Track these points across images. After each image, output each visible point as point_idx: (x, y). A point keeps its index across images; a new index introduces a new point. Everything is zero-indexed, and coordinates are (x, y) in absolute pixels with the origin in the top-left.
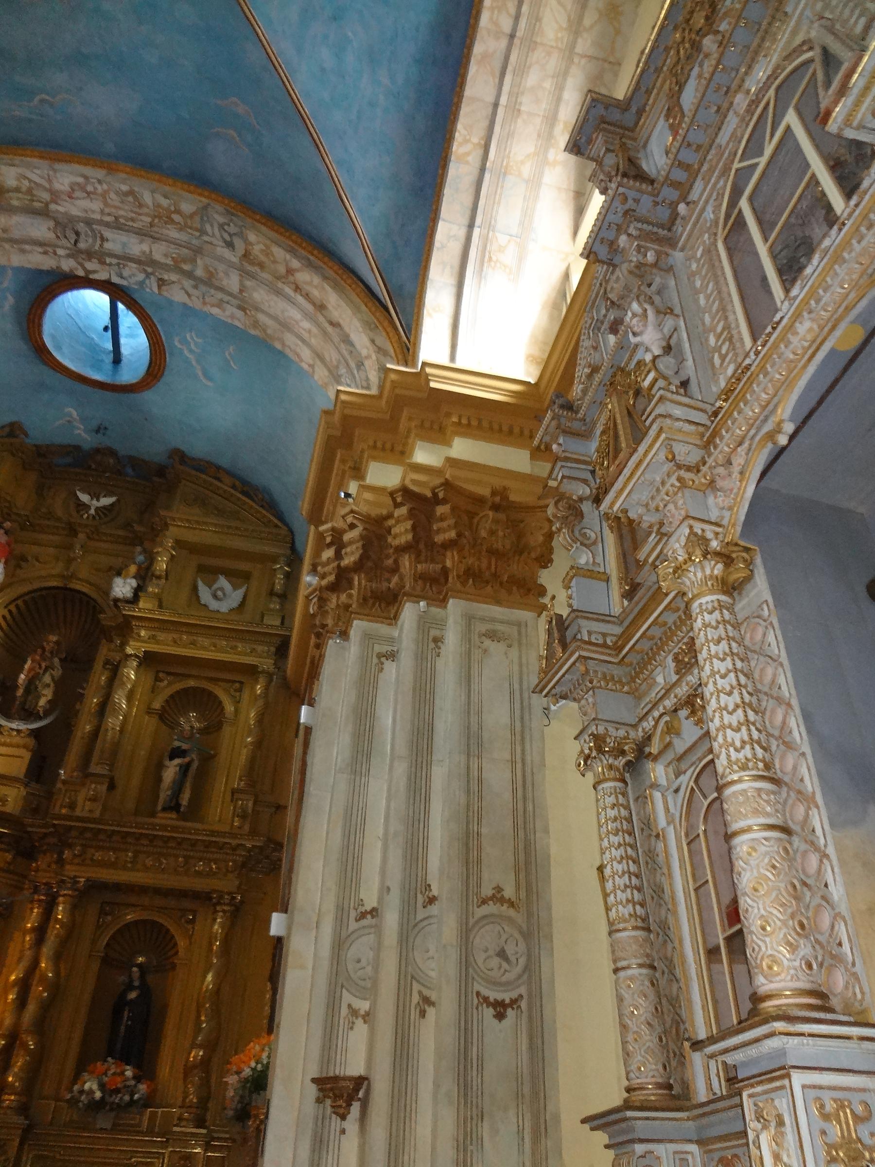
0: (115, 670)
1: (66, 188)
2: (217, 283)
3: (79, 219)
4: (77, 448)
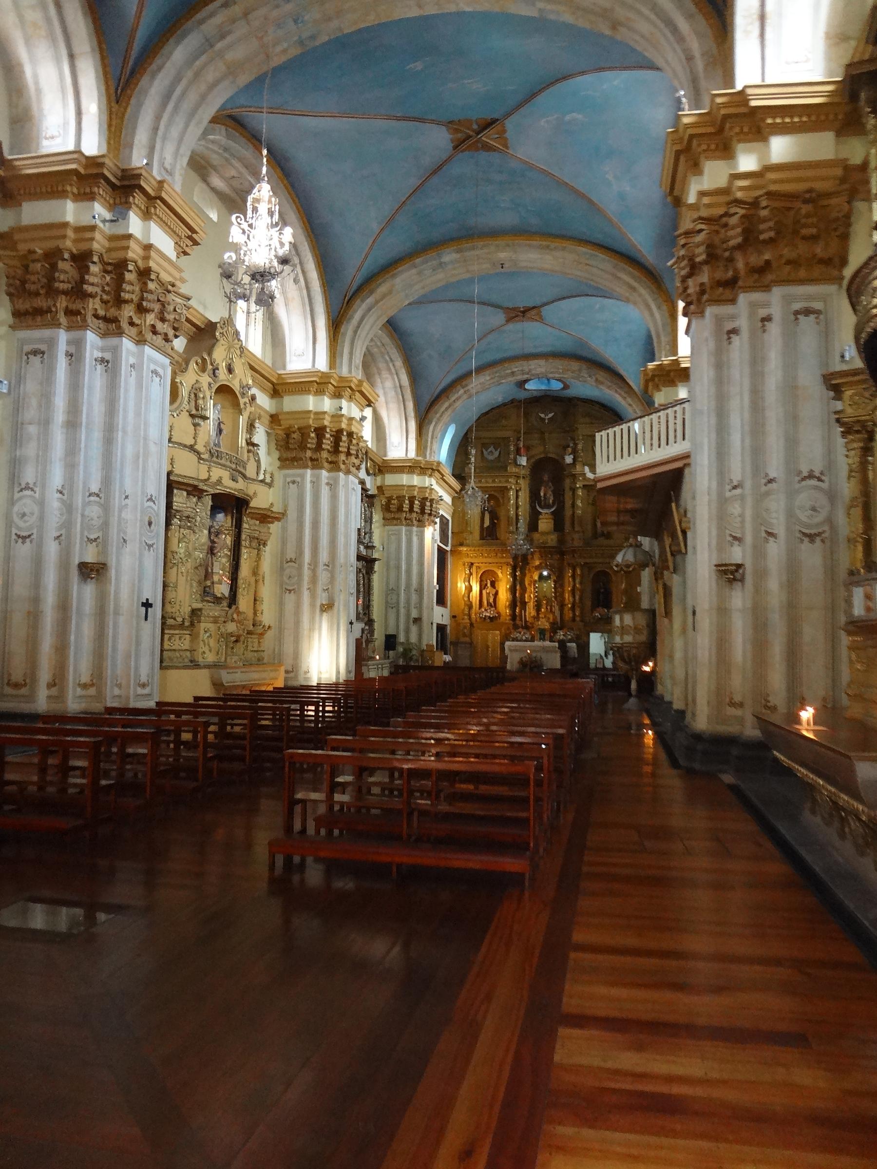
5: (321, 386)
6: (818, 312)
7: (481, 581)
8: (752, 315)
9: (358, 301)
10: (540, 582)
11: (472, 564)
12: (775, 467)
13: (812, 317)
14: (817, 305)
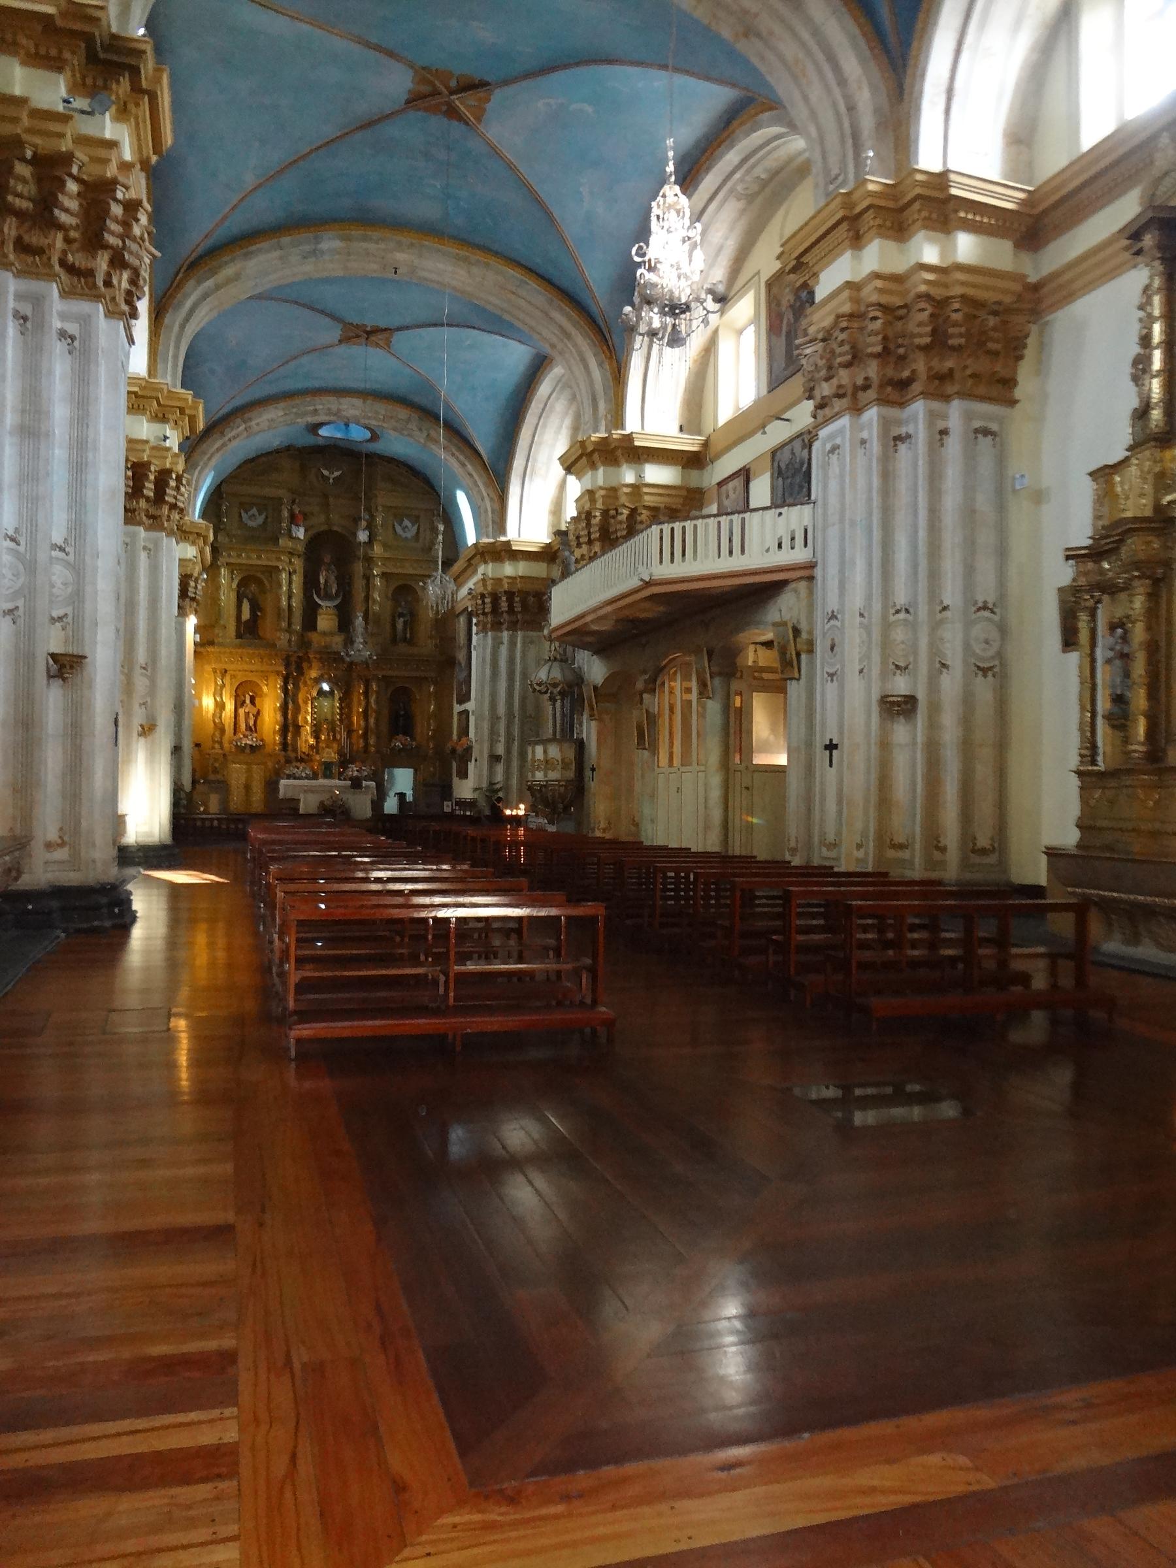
5: (142, 402)
6: (993, 434)
7: (237, 697)
8: (931, 424)
9: (192, 283)
10: (318, 701)
11: (226, 671)
12: (951, 594)
13: (990, 437)
14: (994, 427)
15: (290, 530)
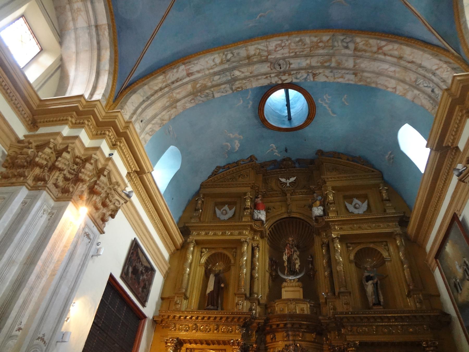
0: (328, 247)
1: (274, 48)
2: (342, 67)
3: (280, 59)
4: (275, 161)
15: (252, 215)
